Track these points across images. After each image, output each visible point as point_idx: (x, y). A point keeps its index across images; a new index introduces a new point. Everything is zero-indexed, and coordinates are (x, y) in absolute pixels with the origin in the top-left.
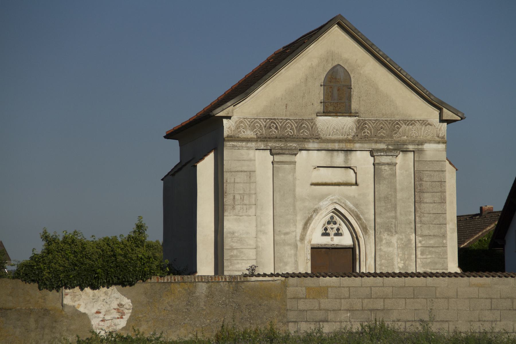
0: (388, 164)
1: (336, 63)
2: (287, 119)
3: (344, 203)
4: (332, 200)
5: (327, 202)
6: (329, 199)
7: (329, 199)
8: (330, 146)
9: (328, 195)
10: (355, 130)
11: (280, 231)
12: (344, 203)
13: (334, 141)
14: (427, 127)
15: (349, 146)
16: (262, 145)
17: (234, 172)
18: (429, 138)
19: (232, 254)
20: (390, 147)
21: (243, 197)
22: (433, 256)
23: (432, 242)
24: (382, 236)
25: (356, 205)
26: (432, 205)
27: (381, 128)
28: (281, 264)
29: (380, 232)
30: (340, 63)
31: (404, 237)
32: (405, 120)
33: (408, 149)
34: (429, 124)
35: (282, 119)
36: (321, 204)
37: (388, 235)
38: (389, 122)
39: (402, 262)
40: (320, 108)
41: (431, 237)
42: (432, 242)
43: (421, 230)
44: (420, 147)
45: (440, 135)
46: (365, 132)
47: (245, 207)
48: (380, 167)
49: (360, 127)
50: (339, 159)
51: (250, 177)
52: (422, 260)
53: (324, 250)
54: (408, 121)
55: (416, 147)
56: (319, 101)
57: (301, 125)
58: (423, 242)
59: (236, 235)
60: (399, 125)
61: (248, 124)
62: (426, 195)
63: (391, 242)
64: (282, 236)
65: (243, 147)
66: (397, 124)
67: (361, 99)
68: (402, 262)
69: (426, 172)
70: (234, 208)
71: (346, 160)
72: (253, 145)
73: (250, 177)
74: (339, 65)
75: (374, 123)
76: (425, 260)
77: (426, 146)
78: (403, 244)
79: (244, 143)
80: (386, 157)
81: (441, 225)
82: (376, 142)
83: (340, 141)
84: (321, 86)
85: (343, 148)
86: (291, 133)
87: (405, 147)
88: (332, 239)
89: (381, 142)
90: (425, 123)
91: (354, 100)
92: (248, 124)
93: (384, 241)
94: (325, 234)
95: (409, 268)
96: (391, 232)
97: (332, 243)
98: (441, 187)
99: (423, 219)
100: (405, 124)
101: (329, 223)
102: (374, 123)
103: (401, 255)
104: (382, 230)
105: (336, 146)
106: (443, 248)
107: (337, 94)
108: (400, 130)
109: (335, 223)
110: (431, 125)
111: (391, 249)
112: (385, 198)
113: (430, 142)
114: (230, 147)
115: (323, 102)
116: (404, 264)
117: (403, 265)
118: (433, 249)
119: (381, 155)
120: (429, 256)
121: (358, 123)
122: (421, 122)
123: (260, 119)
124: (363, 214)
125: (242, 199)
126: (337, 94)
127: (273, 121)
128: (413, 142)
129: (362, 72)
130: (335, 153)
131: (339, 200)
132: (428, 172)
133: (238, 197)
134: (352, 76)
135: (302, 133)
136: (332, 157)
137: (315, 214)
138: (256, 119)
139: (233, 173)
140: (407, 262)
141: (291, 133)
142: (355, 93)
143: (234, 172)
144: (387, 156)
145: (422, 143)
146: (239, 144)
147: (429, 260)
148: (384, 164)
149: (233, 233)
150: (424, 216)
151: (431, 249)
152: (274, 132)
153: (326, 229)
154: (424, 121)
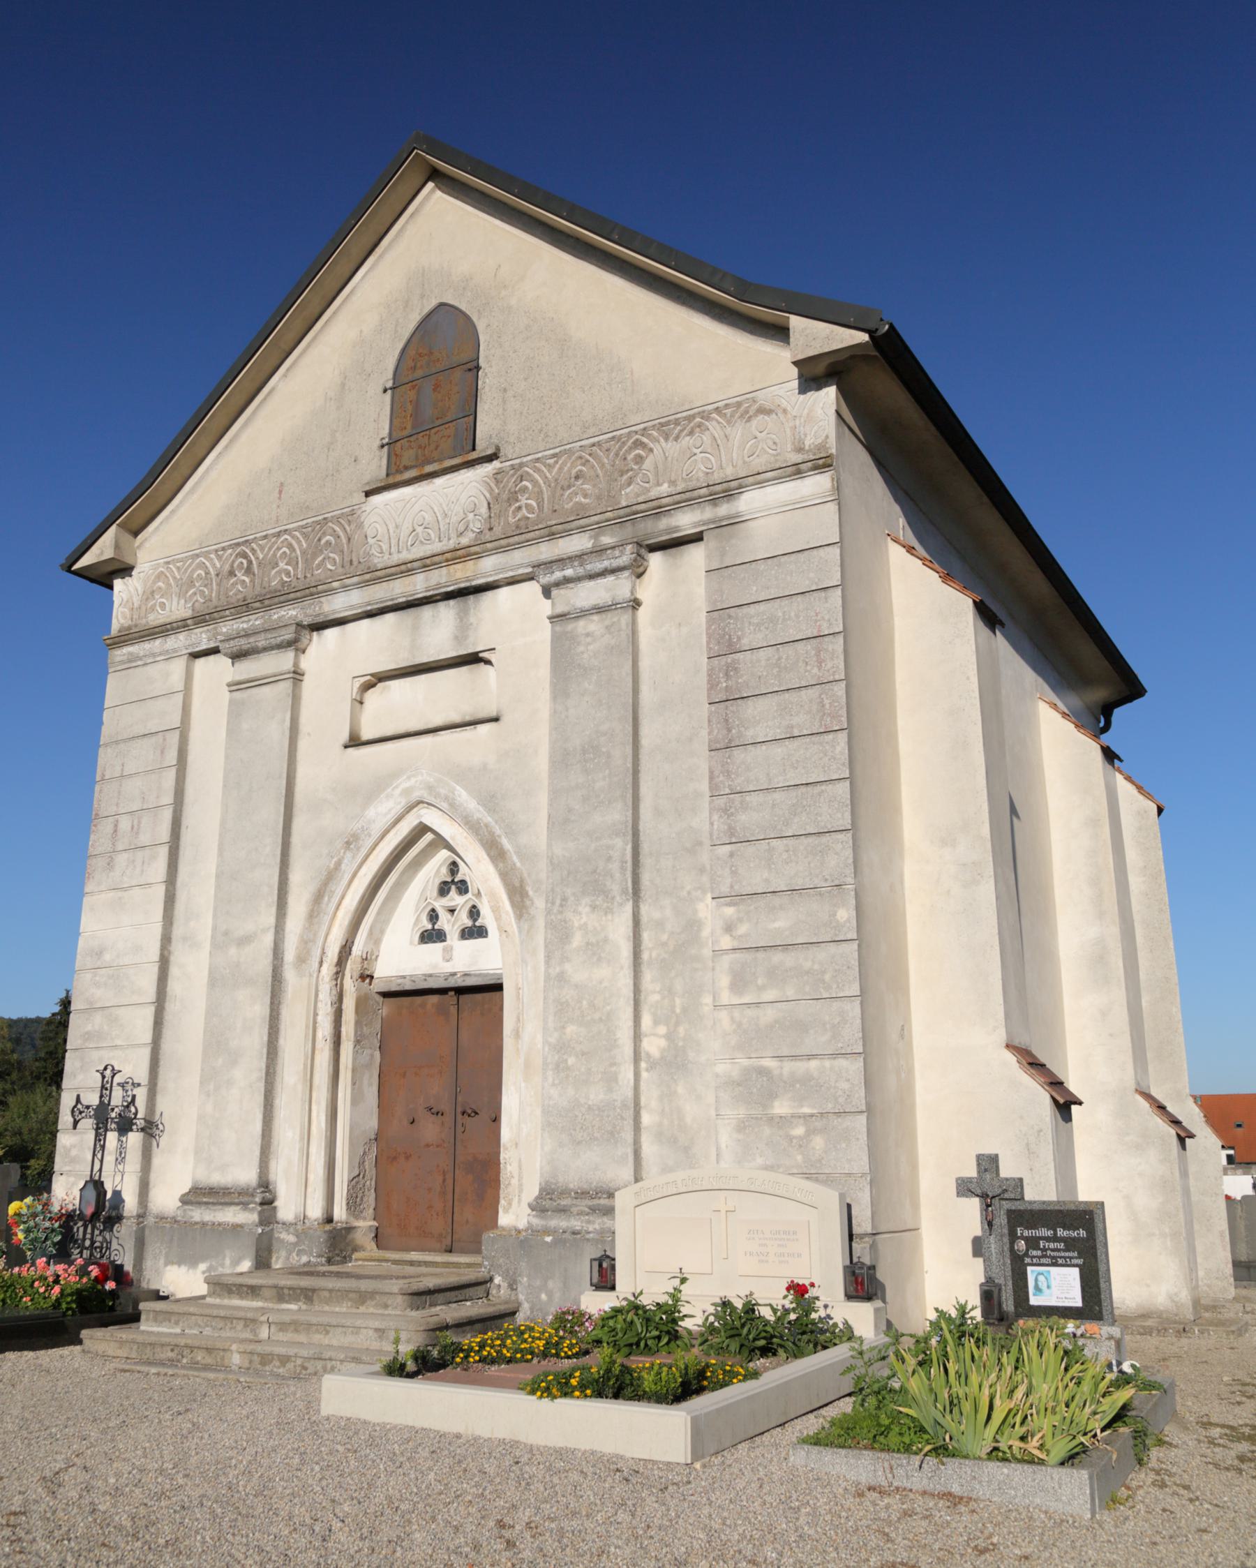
0: (600, 610)
1: (433, 303)
2: (278, 535)
3: (446, 799)
4: (407, 792)
5: (390, 804)
6: (398, 792)
7: (398, 792)
8: (400, 589)
9: (395, 775)
10: (484, 510)
11: (226, 933)
12: (446, 799)
13: (405, 569)
14: (754, 422)
15: (459, 575)
16: (202, 638)
17: (124, 741)
18: (759, 463)
19: (89, 1028)
20: (607, 540)
21: (139, 822)
22: (790, 993)
23: (781, 923)
24: (569, 915)
25: (490, 801)
26: (778, 751)
27: (577, 478)
28: (220, 1061)
29: (564, 899)
30: (444, 300)
31: (668, 912)
32: (668, 423)
33: (677, 529)
34: (763, 411)
35: (265, 537)
36: (371, 812)
37: (594, 908)
38: (605, 446)
39: (662, 1030)
40: (375, 465)
41: (776, 900)
42: (781, 923)
43: (734, 873)
44: (724, 510)
45: (808, 443)
46: (519, 508)
47: (139, 854)
48: (570, 627)
49: (505, 496)
50: (438, 632)
51: (162, 752)
52: (736, 1014)
53: (434, 999)
54: (677, 422)
55: (708, 513)
56: (378, 443)
57: (319, 540)
58: (743, 929)
59: (107, 957)
60: (643, 446)
61: (175, 578)
62: (752, 709)
63: (606, 940)
64: (233, 951)
65: (154, 655)
66: (638, 444)
67: (510, 393)
68: (662, 1030)
69: (752, 610)
70: (110, 865)
71: (463, 629)
72: (180, 642)
73: (162, 752)
74: (442, 305)
75: (550, 467)
76: (750, 1012)
77: (748, 502)
78: (664, 944)
79: (158, 642)
80: (592, 583)
81: (825, 839)
82: (552, 536)
83: (427, 563)
84: (385, 391)
85: (439, 585)
86: (288, 574)
87: (664, 523)
88: (448, 956)
89: (568, 533)
90: (745, 409)
91: (486, 407)
92: (175, 578)
93: (577, 940)
94: (432, 936)
95: (691, 1055)
96: (606, 893)
97: (448, 968)
98: (820, 662)
99: (743, 817)
100: (666, 439)
101: (444, 889)
102: (550, 467)
103: (656, 997)
104: (569, 891)
105: (419, 585)
106: (832, 946)
107: (434, 398)
108: (648, 464)
109: (463, 888)
110: (768, 412)
111: (603, 972)
112: (584, 751)
113: (759, 479)
114: (122, 662)
115: (391, 444)
116: (669, 1037)
117: (663, 1043)
118: (787, 959)
119: (567, 581)
120: (770, 995)
121: (497, 482)
122: (728, 411)
123: (206, 555)
124: (511, 832)
125: (135, 830)
126: (434, 398)
127: (242, 547)
128: (686, 499)
129: (513, 302)
130: (427, 612)
131: (430, 788)
132: (762, 607)
133: (125, 824)
134: (481, 327)
135: (319, 566)
136: (416, 628)
137: (349, 855)
138: (198, 556)
139: (122, 746)
140: (681, 1030)
141: (288, 574)
142: (488, 381)
143: (124, 741)
144: (592, 577)
145: (727, 491)
146: (146, 647)
147: (769, 1014)
148: (584, 613)
149: (100, 953)
150: (745, 807)
151: (777, 957)
152: (242, 585)
153: (433, 916)
154: (739, 404)
